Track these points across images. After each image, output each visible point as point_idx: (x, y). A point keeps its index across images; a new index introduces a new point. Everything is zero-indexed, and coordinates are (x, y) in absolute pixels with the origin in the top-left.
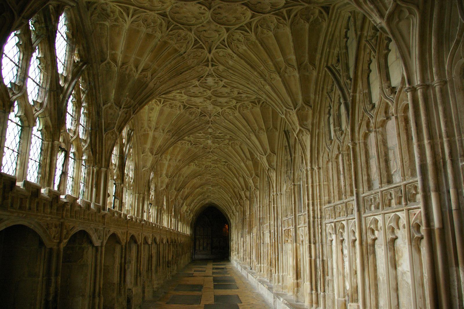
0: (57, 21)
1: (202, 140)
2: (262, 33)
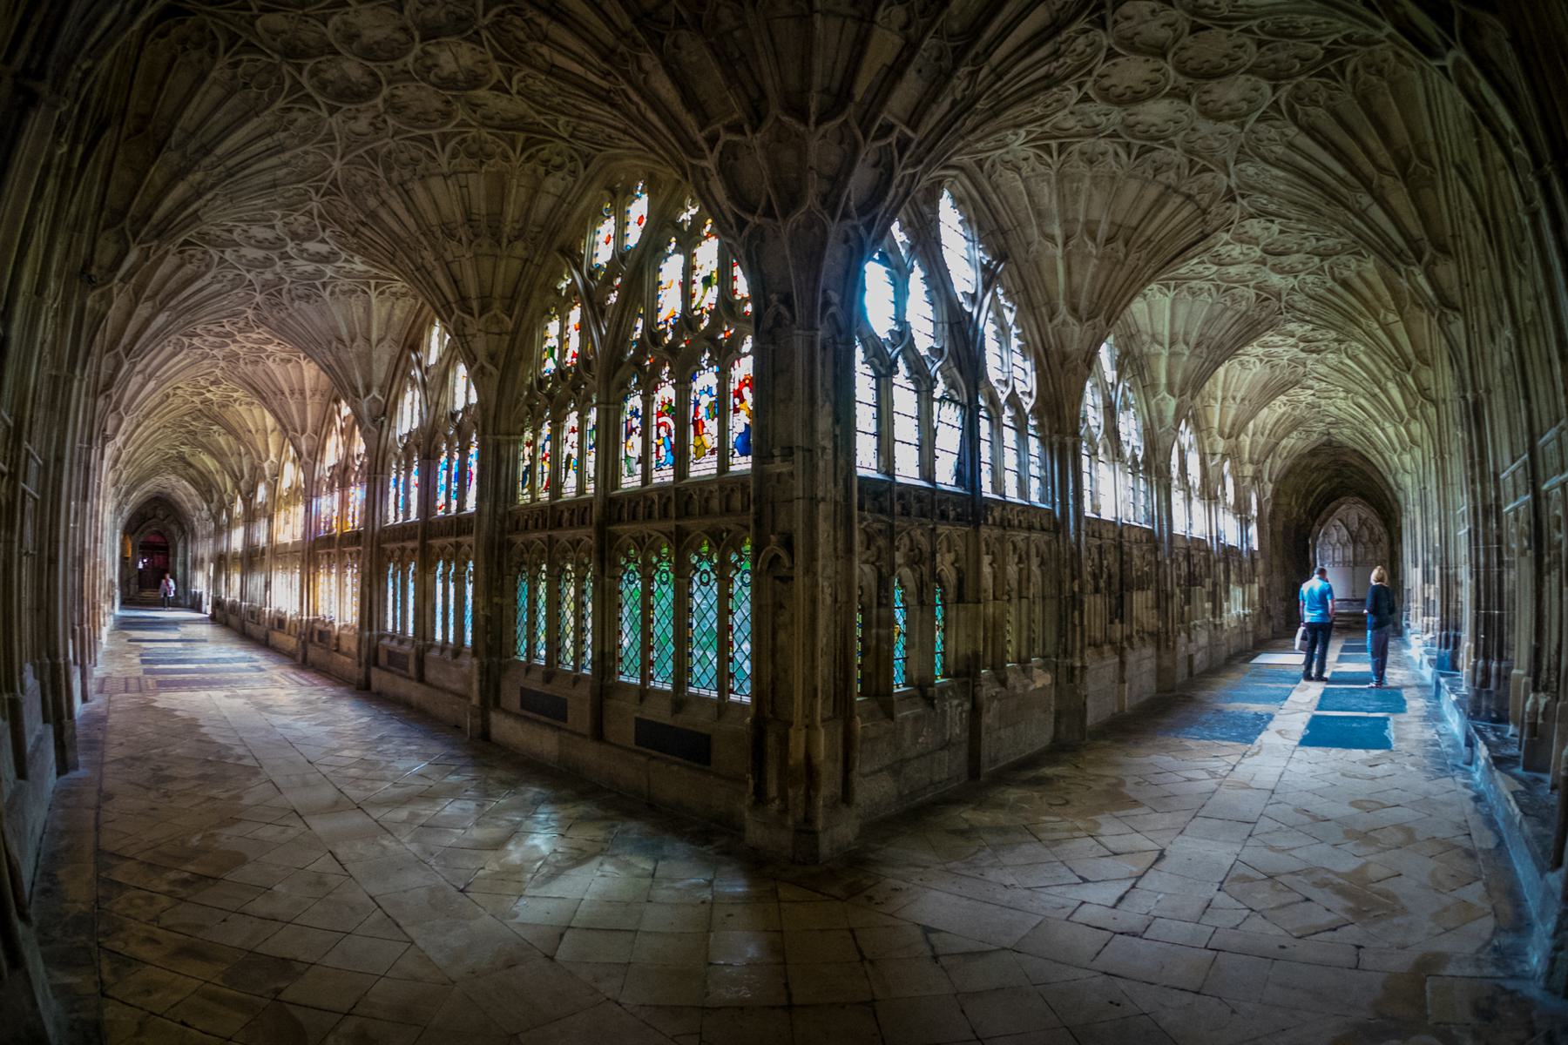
0: (936, 211)
1: (1280, 350)
2: (1307, 115)
